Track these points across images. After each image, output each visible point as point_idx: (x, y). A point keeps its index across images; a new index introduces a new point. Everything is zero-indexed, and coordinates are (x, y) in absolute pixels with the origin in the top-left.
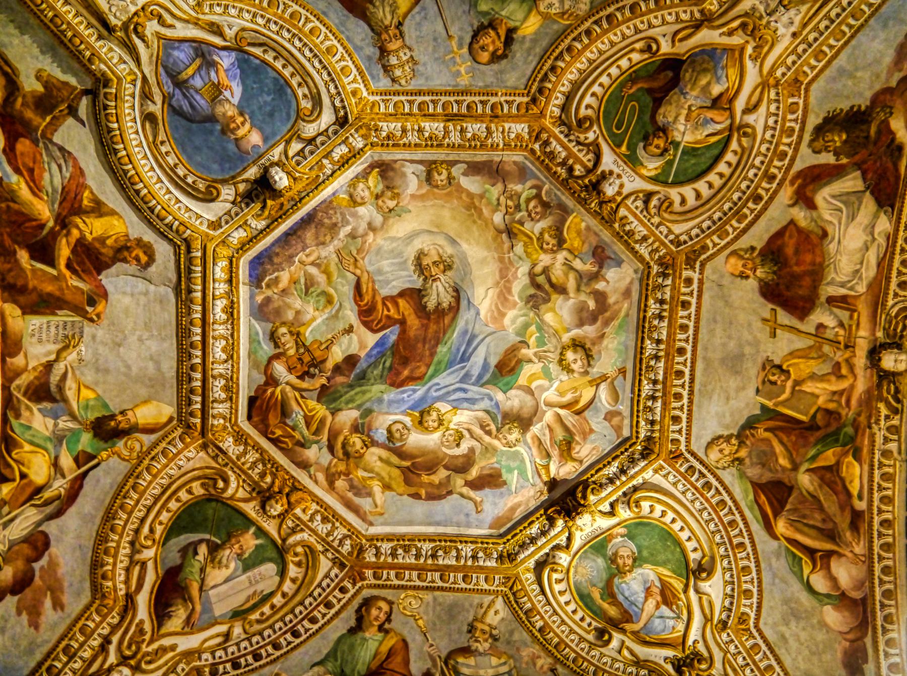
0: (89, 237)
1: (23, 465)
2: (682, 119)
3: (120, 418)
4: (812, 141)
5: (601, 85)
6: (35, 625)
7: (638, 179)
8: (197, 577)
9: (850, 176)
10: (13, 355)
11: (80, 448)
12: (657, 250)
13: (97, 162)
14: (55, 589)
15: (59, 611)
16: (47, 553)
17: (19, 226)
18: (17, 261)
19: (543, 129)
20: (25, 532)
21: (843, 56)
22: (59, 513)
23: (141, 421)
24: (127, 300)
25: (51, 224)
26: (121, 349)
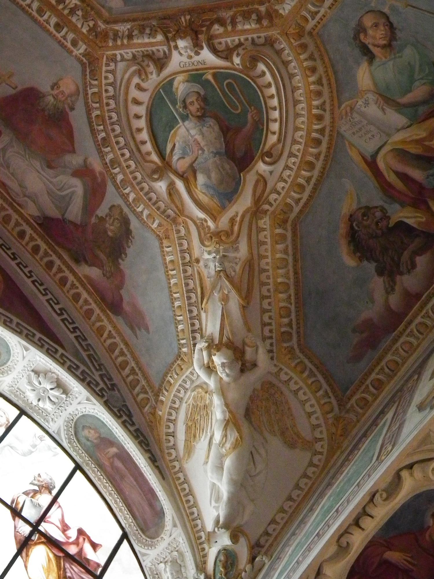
2: (199, 138)
4: (122, 211)
5: (272, 97)
7: (179, 69)
9: (80, 214)
12: (115, 40)
19: (272, 26)
21: (163, 277)
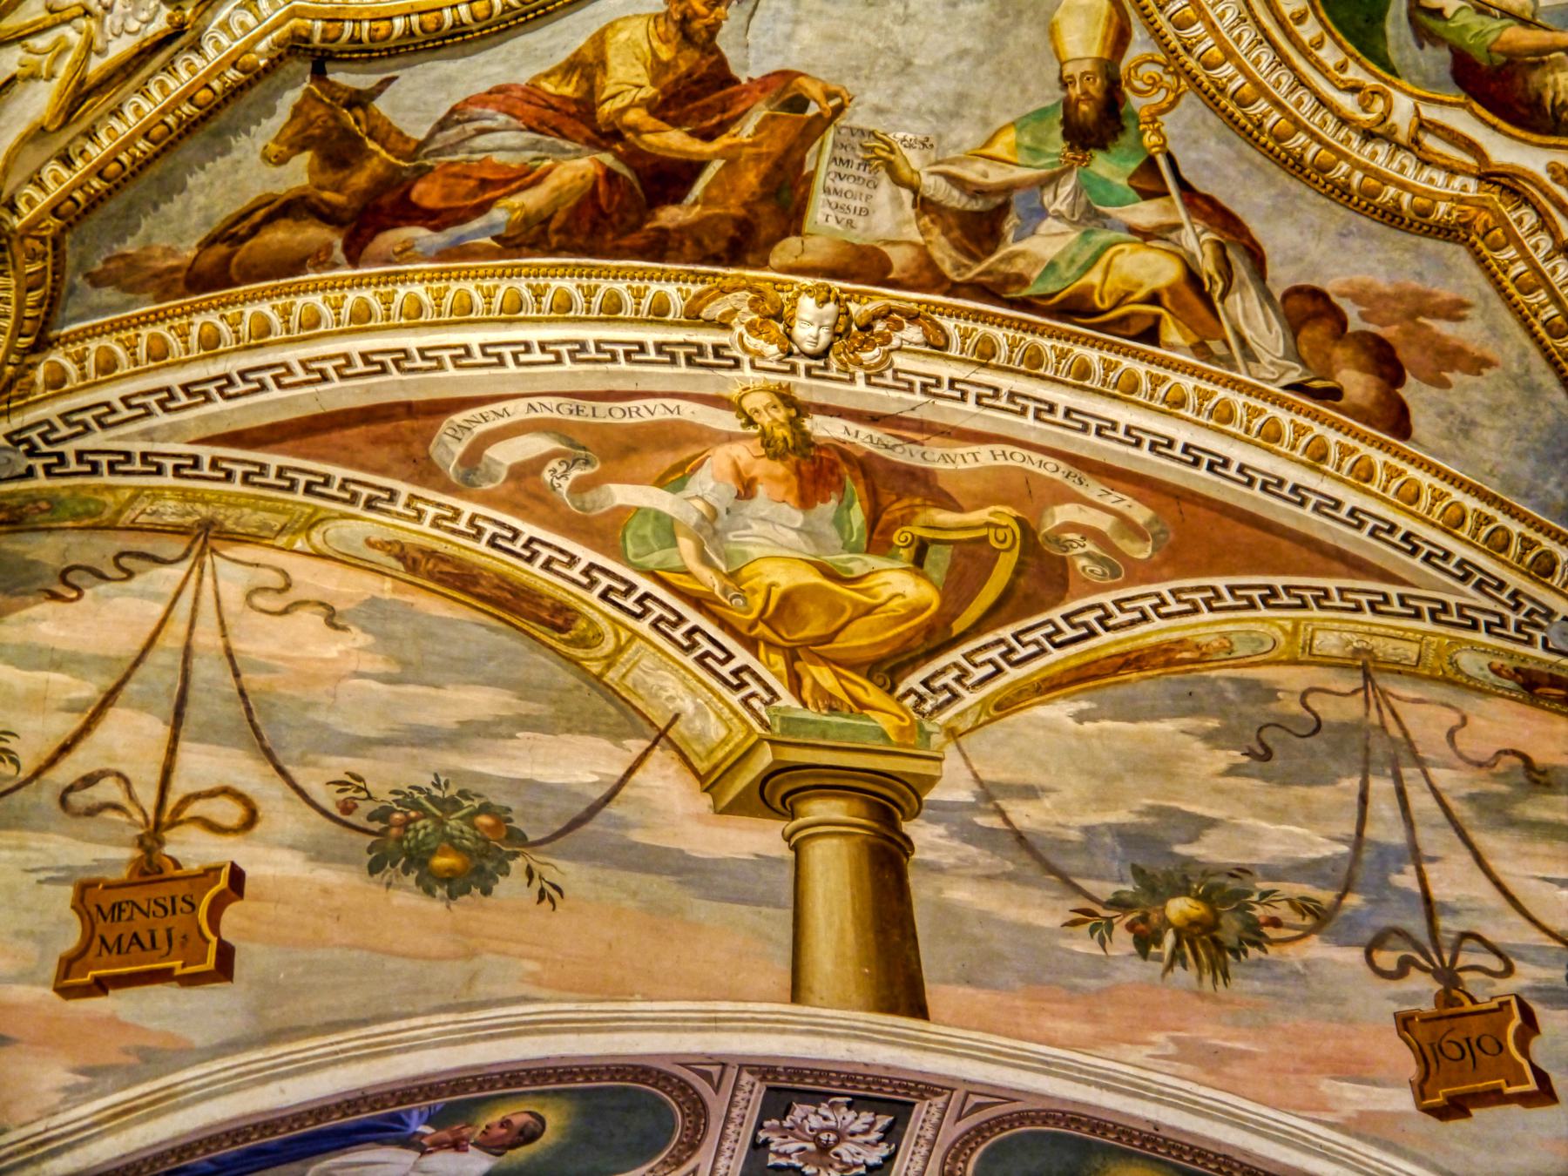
0: (649, 91)
1: (1129, 294)
3: (1075, 91)
6: (1479, 364)
8: (1497, 24)
10: (886, 265)
11: (1122, 182)
13: (481, 58)
14: (1420, 306)
15: (1468, 312)
16: (1335, 299)
17: (606, 216)
18: (681, 229)
20: (1276, 327)
22: (1256, 257)
23: (1095, 51)
24: (806, 34)
25: (608, 159)
26: (917, 61)
